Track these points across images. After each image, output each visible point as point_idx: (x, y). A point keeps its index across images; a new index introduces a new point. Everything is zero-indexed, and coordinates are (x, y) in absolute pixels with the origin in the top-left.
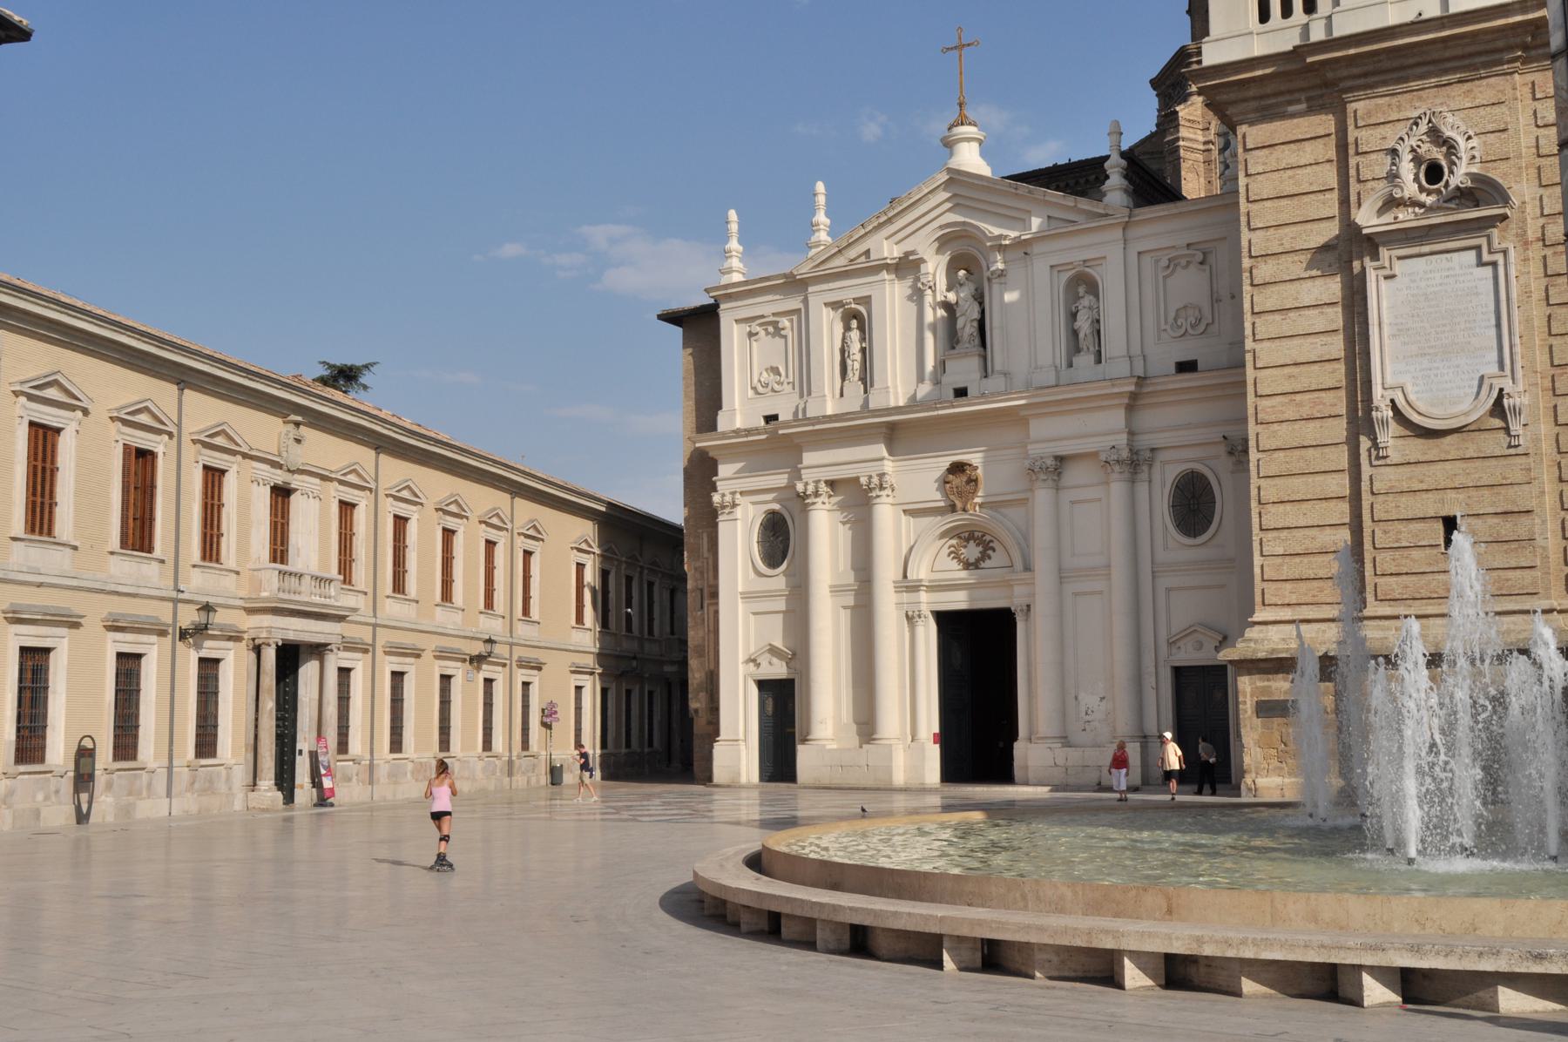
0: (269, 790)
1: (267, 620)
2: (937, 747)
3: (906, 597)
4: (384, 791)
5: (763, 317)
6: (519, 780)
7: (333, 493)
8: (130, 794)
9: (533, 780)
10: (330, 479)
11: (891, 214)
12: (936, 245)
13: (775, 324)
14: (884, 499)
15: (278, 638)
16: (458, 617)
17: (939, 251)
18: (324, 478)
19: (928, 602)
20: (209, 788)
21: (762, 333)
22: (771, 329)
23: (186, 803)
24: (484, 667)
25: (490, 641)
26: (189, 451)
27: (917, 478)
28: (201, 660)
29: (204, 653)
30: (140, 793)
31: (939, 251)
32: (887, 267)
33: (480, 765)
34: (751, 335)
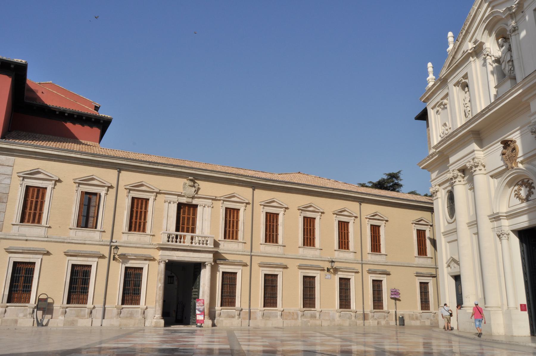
0: (157, 318)
1: (161, 252)
2: (525, 315)
3: (496, 224)
4: (258, 322)
5: (438, 102)
6: (371, 322)
7: (221, 205)
8: (77, 316)
9: (383, 322)
10: (220, 200)
11: (466, 29)
12: (486, 32)
13: (441, 104)
14: (478, 172)
15: (167, 259)
16: (317, 253)
17: (490, 34)
18: (213, 199)
19: (507, 225)
20: (131, 316)
21: (440, 110)
22: (442, 107)
23: (112, 321)
24: (339, 273)
25: (332, 262)
26: (122, 192)
27: (490, 156)
28: (126, 268)
29: (128, 265)
30: (84, 316)
31: (490, 34)
32: (470, 55)
33: (338, 314)
34: (437, 112)
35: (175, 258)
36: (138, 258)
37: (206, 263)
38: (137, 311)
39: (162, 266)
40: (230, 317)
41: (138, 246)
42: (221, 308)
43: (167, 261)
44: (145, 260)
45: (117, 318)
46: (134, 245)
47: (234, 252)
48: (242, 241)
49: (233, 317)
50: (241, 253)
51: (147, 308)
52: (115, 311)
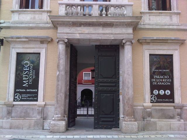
35: (78, 36)
36: (30, 40)
37: (124, 41)
38: (33, 109)
39: (61, 47)
40: (166, 118)
41: (31, 25)
42: (151, 104)
43: (66, 41)
44: (42, 42)
45: (8, 118)
46: (27, 25)
47: (166, 27)
48: (176, 11)
49: (172, 118)
50: (175, 27)
51: (45, 105)
52: (5, 109)
